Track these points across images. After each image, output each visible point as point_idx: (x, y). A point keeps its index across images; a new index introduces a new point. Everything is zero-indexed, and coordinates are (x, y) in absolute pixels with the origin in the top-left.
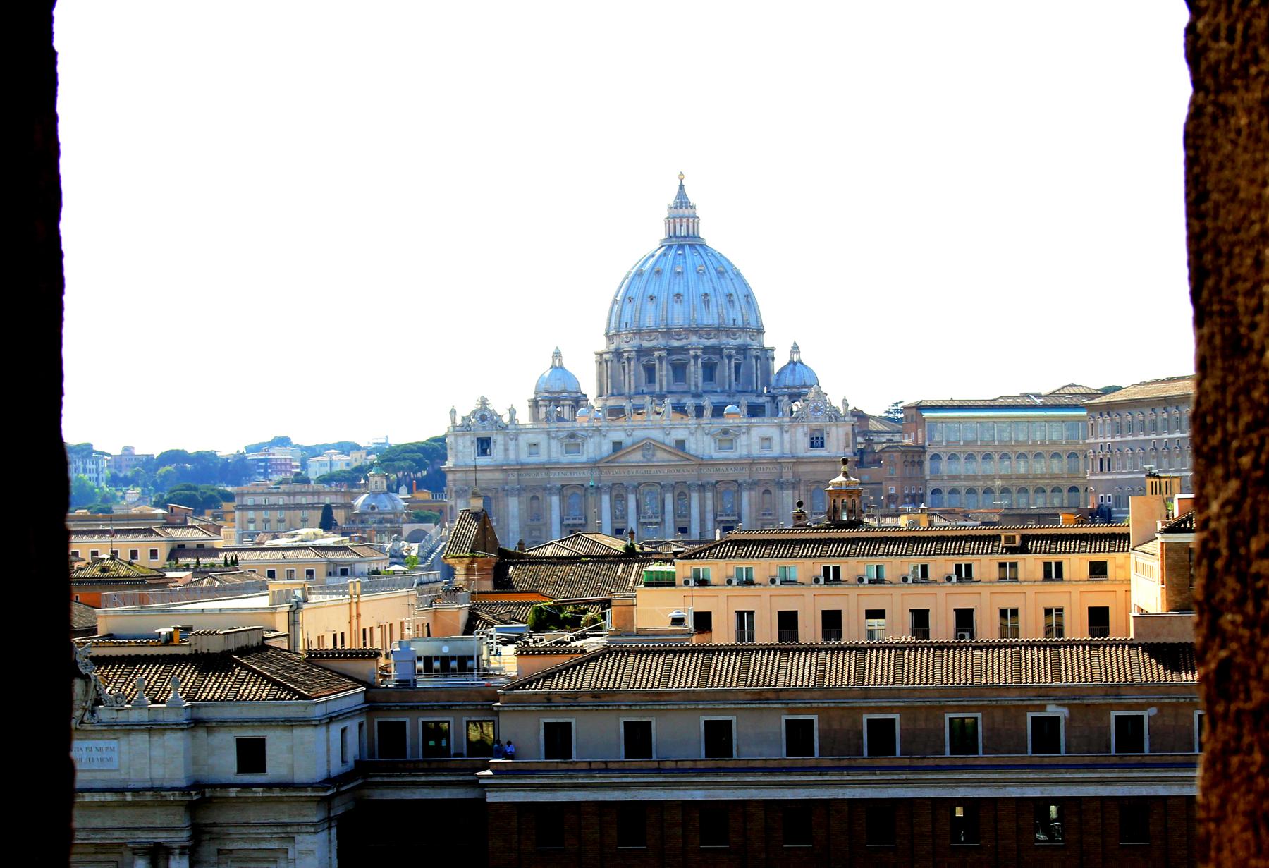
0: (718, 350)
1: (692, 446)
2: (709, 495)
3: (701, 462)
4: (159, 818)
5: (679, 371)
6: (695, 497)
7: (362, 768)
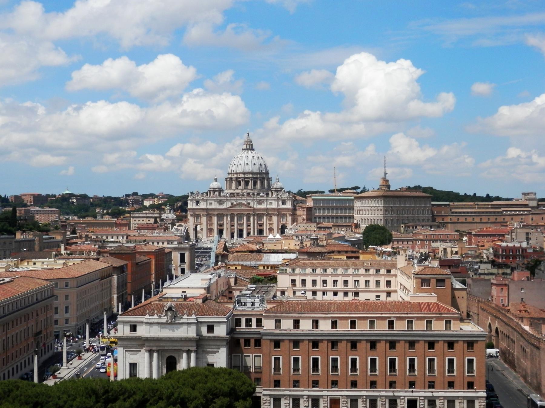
0: (257, 178)
1: (251, 205)
2: (256, 217)
3: (254, 209)
4: (190, 344)
6: (252, 218)
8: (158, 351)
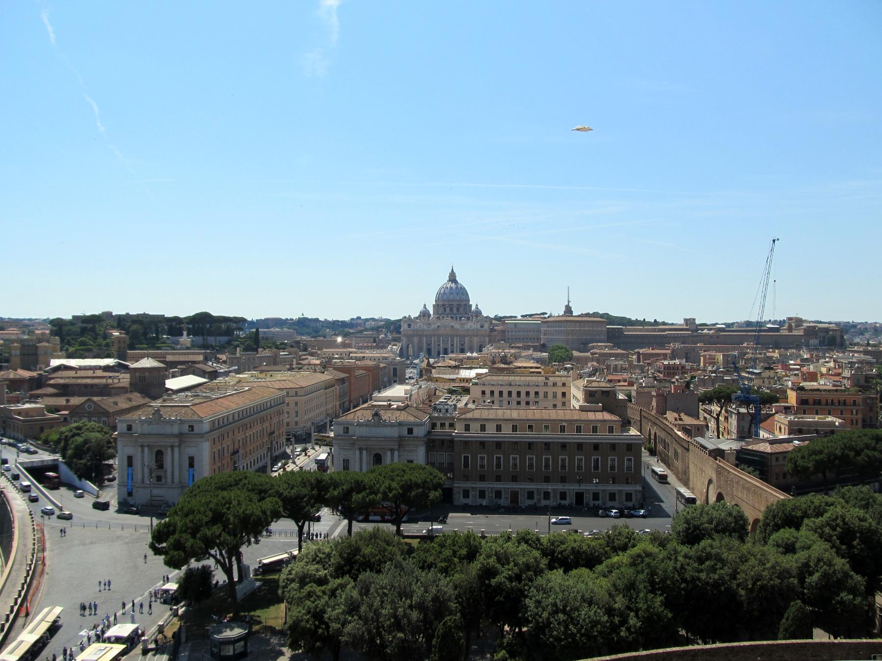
1: (455, 326)
5: (451, 310)
7: (429, 432)
8: (366, 449)
